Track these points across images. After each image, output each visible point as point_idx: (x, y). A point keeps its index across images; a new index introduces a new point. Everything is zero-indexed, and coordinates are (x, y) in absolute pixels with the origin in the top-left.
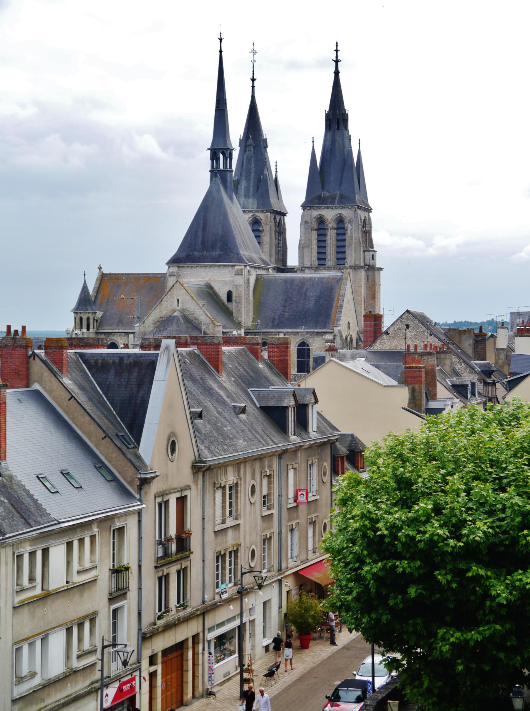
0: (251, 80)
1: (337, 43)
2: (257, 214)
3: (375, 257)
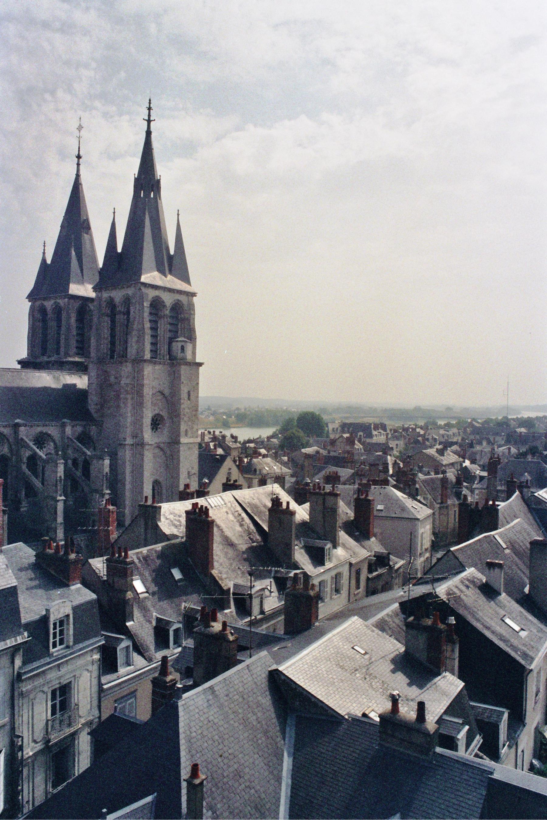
0: (77, 157)
1: (150, 100)
2: (58, 301)
3: (185, 349)
